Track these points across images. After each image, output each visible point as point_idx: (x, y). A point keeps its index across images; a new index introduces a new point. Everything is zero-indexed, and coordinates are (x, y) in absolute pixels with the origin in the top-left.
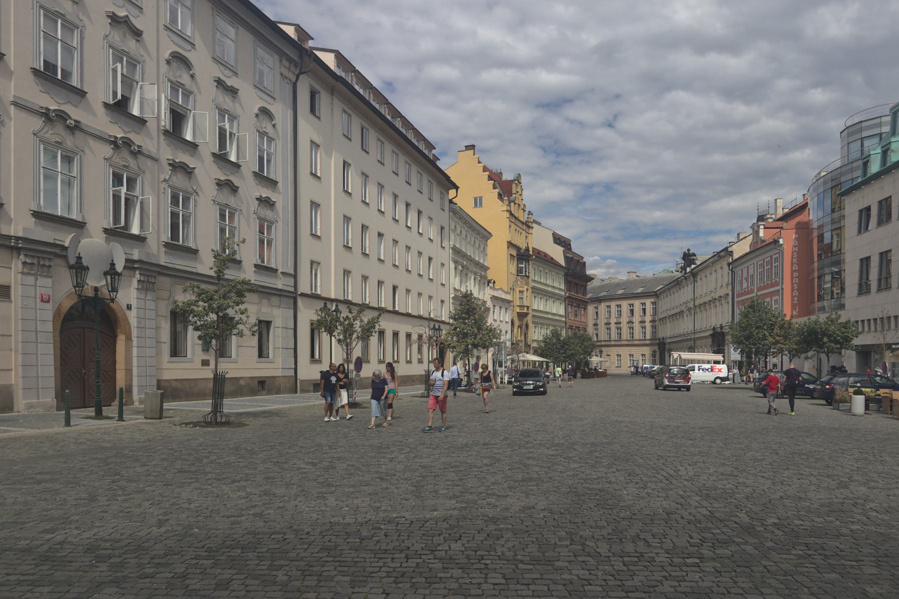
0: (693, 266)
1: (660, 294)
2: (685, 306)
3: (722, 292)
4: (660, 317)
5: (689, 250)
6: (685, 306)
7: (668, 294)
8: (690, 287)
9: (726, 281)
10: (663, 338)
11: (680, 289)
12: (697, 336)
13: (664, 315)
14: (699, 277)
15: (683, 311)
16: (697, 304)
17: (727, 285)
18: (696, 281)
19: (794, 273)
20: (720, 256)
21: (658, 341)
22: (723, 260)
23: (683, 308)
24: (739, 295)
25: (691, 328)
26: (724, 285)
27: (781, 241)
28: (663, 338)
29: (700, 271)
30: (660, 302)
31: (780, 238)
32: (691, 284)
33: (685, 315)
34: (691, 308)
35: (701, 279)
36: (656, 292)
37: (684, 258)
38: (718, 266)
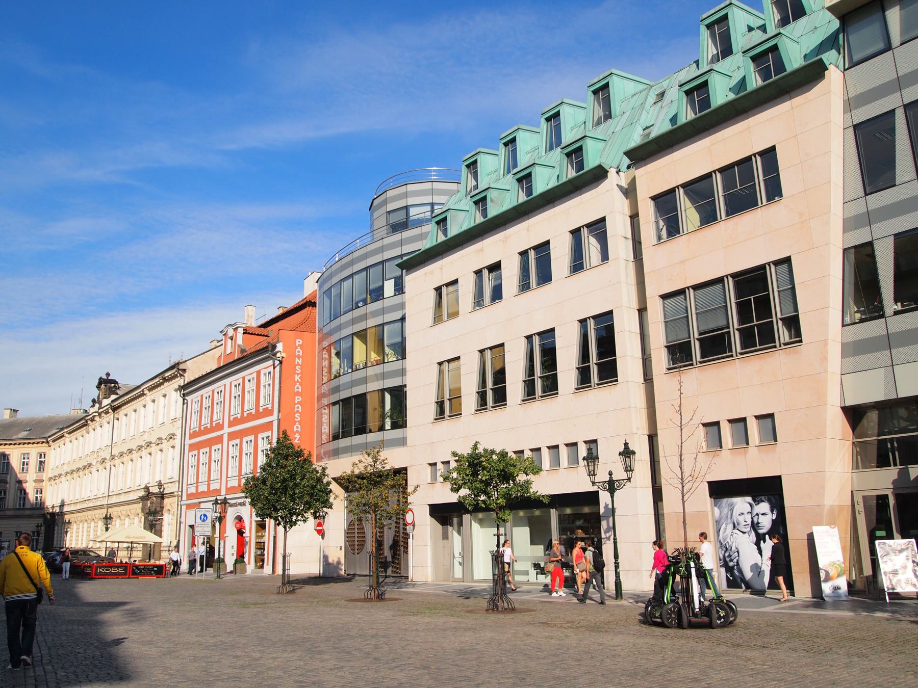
12: (114, 500)
16: (116, 452)
19: (297, 397)
24: (191, 437)
27: (280, 347)
31: (278, 342)
36: (46, 438)
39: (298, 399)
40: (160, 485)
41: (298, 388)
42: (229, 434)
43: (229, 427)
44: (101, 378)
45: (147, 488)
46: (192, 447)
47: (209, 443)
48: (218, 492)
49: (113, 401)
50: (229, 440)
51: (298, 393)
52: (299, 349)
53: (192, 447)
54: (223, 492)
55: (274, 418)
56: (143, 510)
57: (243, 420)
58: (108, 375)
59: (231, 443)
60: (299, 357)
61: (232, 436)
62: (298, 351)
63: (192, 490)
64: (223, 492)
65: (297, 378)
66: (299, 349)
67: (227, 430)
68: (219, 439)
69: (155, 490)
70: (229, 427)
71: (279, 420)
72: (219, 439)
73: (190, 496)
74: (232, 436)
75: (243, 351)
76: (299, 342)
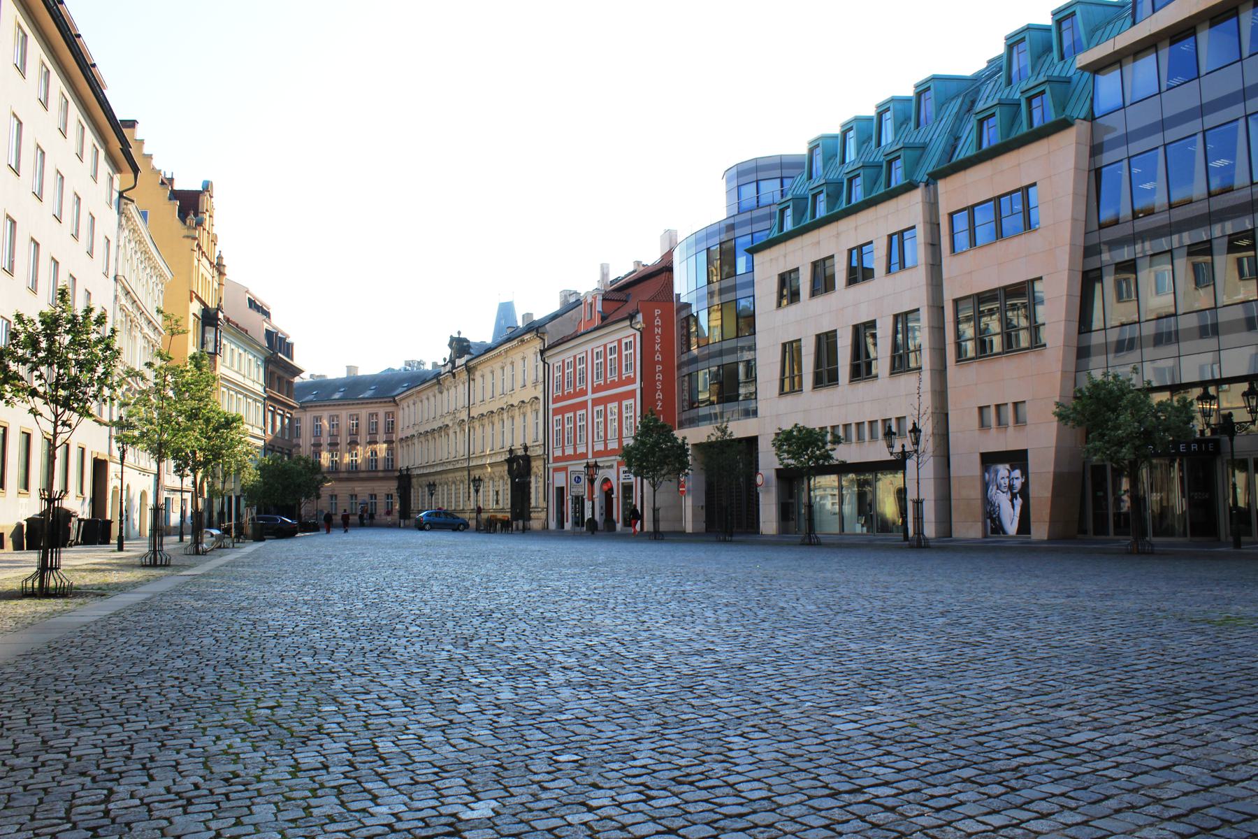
0: (467, 357)
1: (401, 400)
2: (451, 417)
3: (527, 395)
4: (401, 435)
5: (459, 333)
6: (451, 417)
7: (417, 400)
8: (462, 389)
9: (530, 378)
10: (408, 469)
11: (441, 392)
13: (409, 433)
14: (478, 374)
15: (447, 426)
17: (535, 384)
18: (474, 380)
20: (522, 341)
21: (397, 474)
22: (526, 346)
23: (448, 421)
24: (555, 401)
25: (462, 451)
26: (529, 384)
28: (408, 469)
29: (480, 364)
30: (401, 412)
32: (464, 383)
33: (451, 432)
34: (463, 421)
35: (483, 376)
36: (394, 397)
37: (450, 345)
38: (516, 356)
39: (659, 368)
40: (526, 448)
41: (658, 357)
42: (593, 400)
43: (593, 393)
44: (451, 337)
45: (511, 451)
46: (556, 412)
47: (573, 408)
48: (584, 456)
49: (467, 361)
50: (593, 407)
51: (658, 362)
52: (657, 319)
53: (556, 412)
54: (590, 455)
55: (637, 386)
56: (510, 471)
57: (607, 387)
58: (459, 333)
59: (596, 409)
60: (658, 326)
61: (596, 402)
62: (658, 322)
63: (558, 453)
64: (590, 455)
65: (657, 347)
66: (657, 319)
67: (590, 396)
68: (583, 405)
69: (520, 452)
70: (593, 393)
71: (641, 389)
72: (583, 405)
73: (556, 459)
74: (596, 402)
75: (603, 319)
76: (657, 312)
